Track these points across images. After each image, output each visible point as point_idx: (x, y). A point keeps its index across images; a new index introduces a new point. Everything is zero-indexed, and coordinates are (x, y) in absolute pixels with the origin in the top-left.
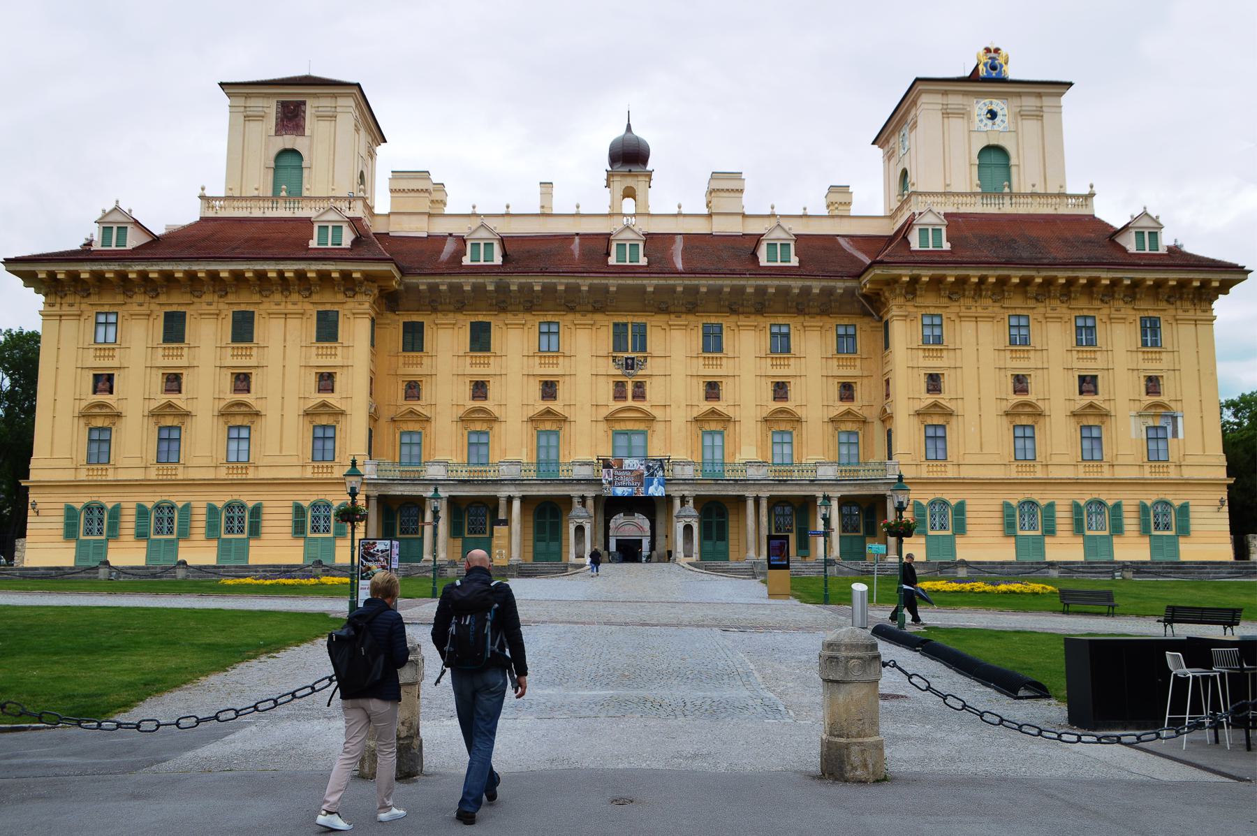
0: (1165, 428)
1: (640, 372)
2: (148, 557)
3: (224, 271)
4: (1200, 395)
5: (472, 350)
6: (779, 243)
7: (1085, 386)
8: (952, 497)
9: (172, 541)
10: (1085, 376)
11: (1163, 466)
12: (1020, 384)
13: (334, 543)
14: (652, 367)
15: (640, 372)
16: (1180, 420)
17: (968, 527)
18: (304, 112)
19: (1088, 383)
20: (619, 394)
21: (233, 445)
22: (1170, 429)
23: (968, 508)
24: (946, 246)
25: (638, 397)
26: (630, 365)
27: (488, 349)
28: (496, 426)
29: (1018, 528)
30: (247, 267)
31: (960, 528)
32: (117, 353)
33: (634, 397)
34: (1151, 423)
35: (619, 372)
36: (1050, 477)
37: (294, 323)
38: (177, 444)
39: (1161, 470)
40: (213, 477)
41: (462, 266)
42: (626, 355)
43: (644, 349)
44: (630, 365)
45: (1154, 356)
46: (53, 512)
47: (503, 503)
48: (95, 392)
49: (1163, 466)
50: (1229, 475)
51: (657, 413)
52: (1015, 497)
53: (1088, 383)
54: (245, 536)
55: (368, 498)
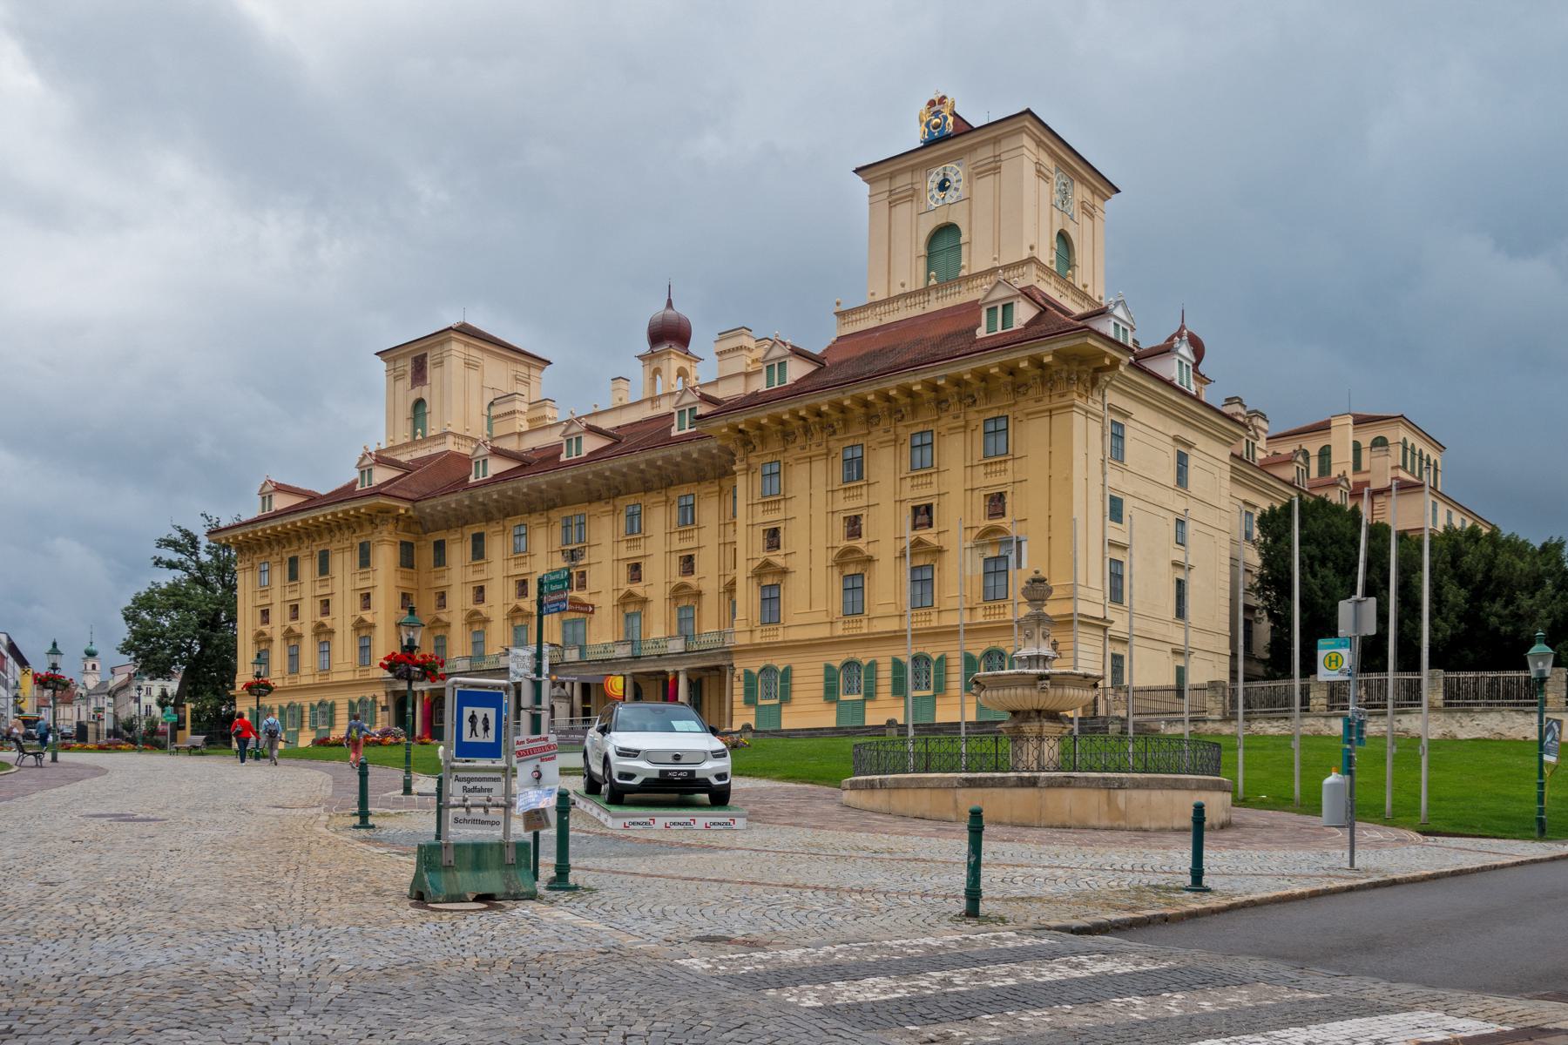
0: (1006, 558)
1: (581, 563)
2: (838, 720)
4: (1050, 509)
5: (473, 559)
6: (687, 409)
7: (920, 519)
8: (780, 663)
10: (919, 507)
11: (999, 607)
12: (854, 526)
13: (864, 706)
15: (581, 563)
16: (1024, 545)
17: (794, 695)
19: (923, 514)
22: (1013, 558)
23: (795, 674)
25: (581, 586)
28: (489, 625)
29: (910, 687)
31: (786, 697)
33: (577, 587)
34: (990, 553)
36: (944, 624)
39: (997, 612)
41: (559, 463)
42: (570, 547)
45: (998, 467)
46: (807, 680)
49: (999, 607)
52: (837, 659)
53: (923, 514)
55: (387, 694)
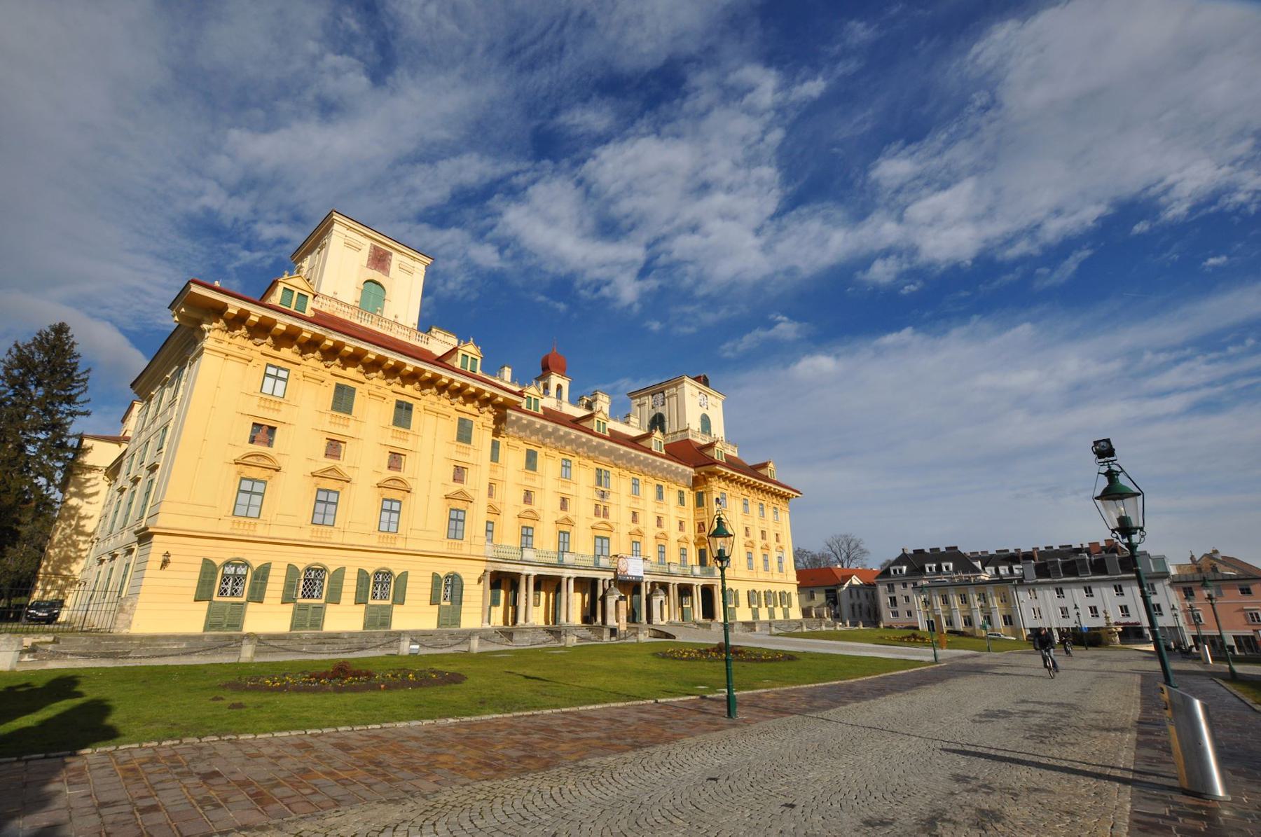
3: (410, 366)
9: (242, 604)
14: (612, 498)
18: (390, 260)
20: (597, 514)
21: (386, 515)
24: (724, 461)
26: (603, 495)
27: (535, 470)
30: (430, 369)
32: (283, 407)
35: (598, 499)
37: (442, 421)
38: (397, 515)
40: (404, 547)
43: (607, 486)
44: (603, 495)
47: (564, 580)
48: (252, 441)
50: (798, 580)
51: (615, 526)
54: (389, 602)
